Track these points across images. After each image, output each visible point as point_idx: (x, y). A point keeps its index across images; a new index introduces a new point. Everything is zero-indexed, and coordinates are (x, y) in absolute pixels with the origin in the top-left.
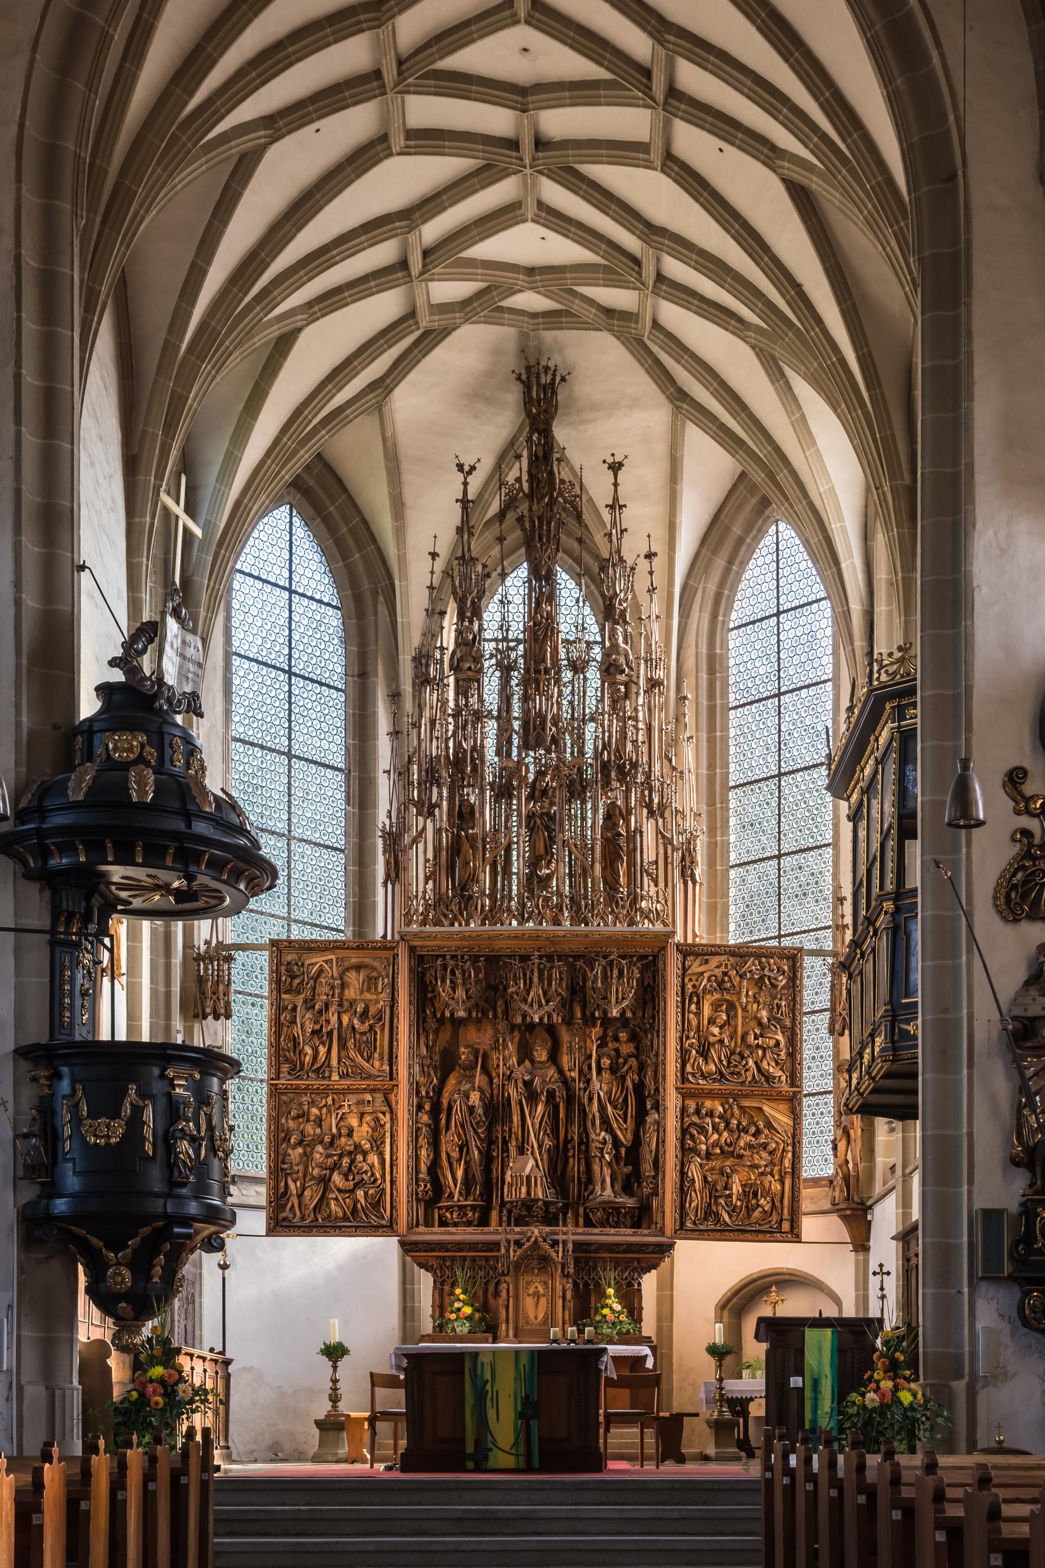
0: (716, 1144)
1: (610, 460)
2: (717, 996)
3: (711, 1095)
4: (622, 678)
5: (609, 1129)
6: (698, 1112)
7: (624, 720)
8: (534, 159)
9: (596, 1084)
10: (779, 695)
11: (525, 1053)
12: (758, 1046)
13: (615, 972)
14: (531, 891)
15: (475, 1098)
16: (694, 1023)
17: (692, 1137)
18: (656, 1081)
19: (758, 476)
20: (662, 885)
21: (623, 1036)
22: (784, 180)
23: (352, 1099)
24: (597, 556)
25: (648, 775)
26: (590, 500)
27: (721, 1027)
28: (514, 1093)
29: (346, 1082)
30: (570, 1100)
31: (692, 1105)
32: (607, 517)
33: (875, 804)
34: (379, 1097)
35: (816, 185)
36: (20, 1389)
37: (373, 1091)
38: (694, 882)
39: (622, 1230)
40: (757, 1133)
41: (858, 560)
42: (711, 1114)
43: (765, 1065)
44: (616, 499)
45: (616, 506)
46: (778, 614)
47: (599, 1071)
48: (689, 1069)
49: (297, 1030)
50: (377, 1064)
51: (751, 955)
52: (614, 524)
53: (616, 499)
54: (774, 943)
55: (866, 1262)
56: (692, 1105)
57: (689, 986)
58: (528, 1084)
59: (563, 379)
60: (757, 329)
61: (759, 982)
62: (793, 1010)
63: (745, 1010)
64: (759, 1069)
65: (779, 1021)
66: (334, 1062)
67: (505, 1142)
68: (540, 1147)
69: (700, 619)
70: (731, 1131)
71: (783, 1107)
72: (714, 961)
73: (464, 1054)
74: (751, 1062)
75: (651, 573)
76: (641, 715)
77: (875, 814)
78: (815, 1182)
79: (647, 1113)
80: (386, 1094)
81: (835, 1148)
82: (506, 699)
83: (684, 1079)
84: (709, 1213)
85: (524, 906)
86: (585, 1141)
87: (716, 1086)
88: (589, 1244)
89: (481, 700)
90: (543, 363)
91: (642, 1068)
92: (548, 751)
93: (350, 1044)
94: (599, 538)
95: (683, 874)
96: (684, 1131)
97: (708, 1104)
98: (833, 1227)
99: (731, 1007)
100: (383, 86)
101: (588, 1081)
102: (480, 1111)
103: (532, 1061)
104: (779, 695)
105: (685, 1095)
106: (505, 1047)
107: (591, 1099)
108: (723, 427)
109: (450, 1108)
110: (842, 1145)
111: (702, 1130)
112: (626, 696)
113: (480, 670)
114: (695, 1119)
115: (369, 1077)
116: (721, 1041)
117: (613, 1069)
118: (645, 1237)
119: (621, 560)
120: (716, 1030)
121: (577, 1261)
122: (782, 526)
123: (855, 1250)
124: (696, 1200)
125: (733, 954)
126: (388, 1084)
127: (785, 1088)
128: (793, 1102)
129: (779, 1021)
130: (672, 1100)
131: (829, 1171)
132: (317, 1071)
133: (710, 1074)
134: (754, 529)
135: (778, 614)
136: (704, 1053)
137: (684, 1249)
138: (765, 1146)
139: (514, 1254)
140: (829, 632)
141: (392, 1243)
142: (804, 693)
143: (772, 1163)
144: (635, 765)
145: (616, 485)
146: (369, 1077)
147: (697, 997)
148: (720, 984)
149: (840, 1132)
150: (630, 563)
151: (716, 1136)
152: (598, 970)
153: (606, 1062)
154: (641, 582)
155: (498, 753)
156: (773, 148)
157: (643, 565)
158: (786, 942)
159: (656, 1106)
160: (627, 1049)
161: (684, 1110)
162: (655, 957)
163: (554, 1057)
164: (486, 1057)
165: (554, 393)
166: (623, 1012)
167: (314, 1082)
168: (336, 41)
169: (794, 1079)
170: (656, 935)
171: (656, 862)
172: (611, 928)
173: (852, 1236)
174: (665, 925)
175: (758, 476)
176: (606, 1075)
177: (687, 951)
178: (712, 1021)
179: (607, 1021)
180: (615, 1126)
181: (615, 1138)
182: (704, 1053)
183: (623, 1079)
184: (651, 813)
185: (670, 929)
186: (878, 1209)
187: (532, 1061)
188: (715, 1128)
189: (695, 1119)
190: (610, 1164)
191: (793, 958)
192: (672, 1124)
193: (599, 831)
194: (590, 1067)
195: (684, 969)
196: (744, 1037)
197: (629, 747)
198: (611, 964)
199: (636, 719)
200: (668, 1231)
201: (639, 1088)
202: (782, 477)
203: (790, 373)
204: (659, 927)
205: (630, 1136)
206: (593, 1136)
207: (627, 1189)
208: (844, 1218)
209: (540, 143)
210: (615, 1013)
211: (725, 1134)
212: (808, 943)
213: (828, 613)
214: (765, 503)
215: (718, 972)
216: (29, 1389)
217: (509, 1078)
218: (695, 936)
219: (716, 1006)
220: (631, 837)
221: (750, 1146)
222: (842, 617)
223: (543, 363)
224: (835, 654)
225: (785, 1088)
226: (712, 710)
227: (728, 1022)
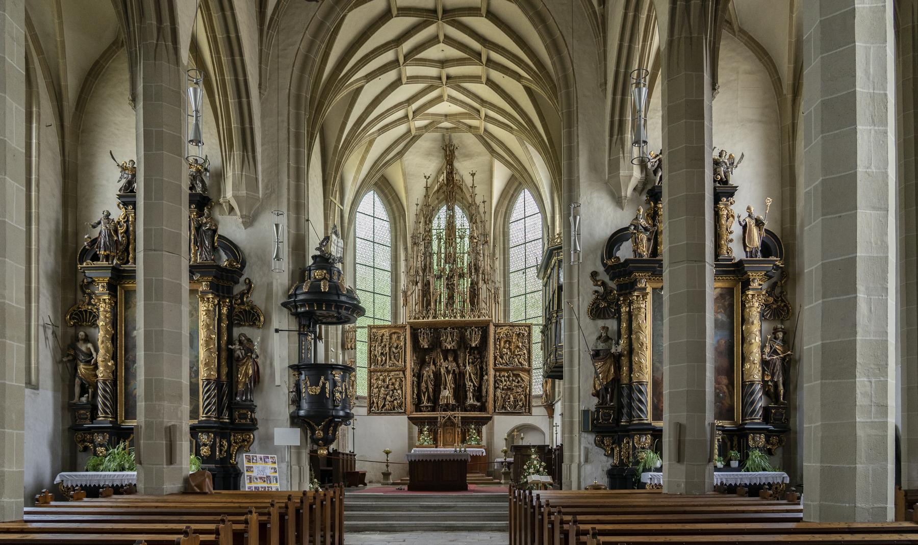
0: (505, 385)
3: (504, 370)
4: (475, 241)
5: (472, 382)
6: (500, 376)
8: (446, 82)
9: (468, 368)
10: (525, 243)
11: (446, 359)
12: (518, 355)
13: (474, 333)
14: (447, 308)
16: (498, 347)
17: (498, 384)
18: (486, 366)
19: (518, 175)
20: (488, 304)
22: (523, 86)
24: (468, 202)
28: (443, 371)
33: (551, 281)
35: (534, 87)
36: (291, 467)
38: (498, 303)
39: (476, 413)
40: (518, 382)
41: (549, 201)
42: (504, 376)
43: (520, 360)
46: (525, 218)
47: (469, 363)
49: (376, 353)
51: (516, 326)
54: (524, 322)
55: (553, 421)
57: (497, 336)
60: (516, 130)
61: (518, 335)
62: (529, 343)
64: (519, 362)
65: (525, 346)
69: (500, 220)
70: (510, 381)
72: (505, 328)
76: (481, 252)
77: (551, 284)
78: (537, 397)
79: (484, 376)
80: (404, 372)
81: (543, 386)
82: (439, 247)
83: (495, 365)
84: (504, 407)
85: (445, 312)
88: (465, 417)
89: (432, 249)
91: (482, 362)
92: (453, 264)
94: (468, 196)
96: (495, 382)
97: (503, 374)
98: (543, 411)
99: (510, 343)
100: (399, 64)
101: (465, 367)
103: (448, 361)
104: (525, 243)
105: (496, 370)
108: (506, 161)
111: (502, 382)
113: (431, 240)
116: (507, 353)
117: (473, 363)
118: (483, 415)
121: (462, 423)
122: (526, 190)
123: (549, 418)
124: (499, 404)
125: (511, 326)
127: (527, 367)
128: (529, 372)
129: (525, 346)
130: (492, 372)
131: (541, 393)
133: (504, 363)
134: (517, 191)
135: (525, 218)
136: (502, 358)
137: (497, 418)
138: (521, 386)
139: (443, 421)
140: (541, 223)
141: (404, 419)
142: (533, 242)
143: (523, 391)
147: (500, 339)
148: (506, 335)
150: (478, 204)
152: (468, 332)
154: (481, 210)
155: (437, 265)
156: (520, 75)
157: (482, 205)
158: (528, 322)
159: (487, 374)
161: (495, 375)
166: (476, 345)
168: (385, 53)
169: (530, 365)
172: (472, 319)
173: (548, 414)
174: (489, 317)
175: (518, 175)
177: (496, 326)
179: (472, 348)
181: (474, 384)
182: (502, 358)
184: (485, 282)
185: (490, 319)
186: (556, 405)
188: (505, 381)
191: (529, 327)
193: (468, 289)
195: (495, 331)
196: (514, 352)
198: (472, 330)
200: (491, 413)
201: (481, 368)
202: (525, 175)
203: (527, 144)
204: (487, 318)
205: (478, 383)
207: (478, 400)
208: (545, 408)
209: (448, 77)
210: (473, 345)
212: (534, 321)
213: (540, 217)
214: (520, 183)
215: (506, 332)
216: (293, 467)
217: (441, 366)
218: (499, 320)
219: (505, 342)
221: (516, 386)
222: (545, 218)
224: (543, 230)
225: (527, 367)
226: (504, 248)
227: (509, 348)
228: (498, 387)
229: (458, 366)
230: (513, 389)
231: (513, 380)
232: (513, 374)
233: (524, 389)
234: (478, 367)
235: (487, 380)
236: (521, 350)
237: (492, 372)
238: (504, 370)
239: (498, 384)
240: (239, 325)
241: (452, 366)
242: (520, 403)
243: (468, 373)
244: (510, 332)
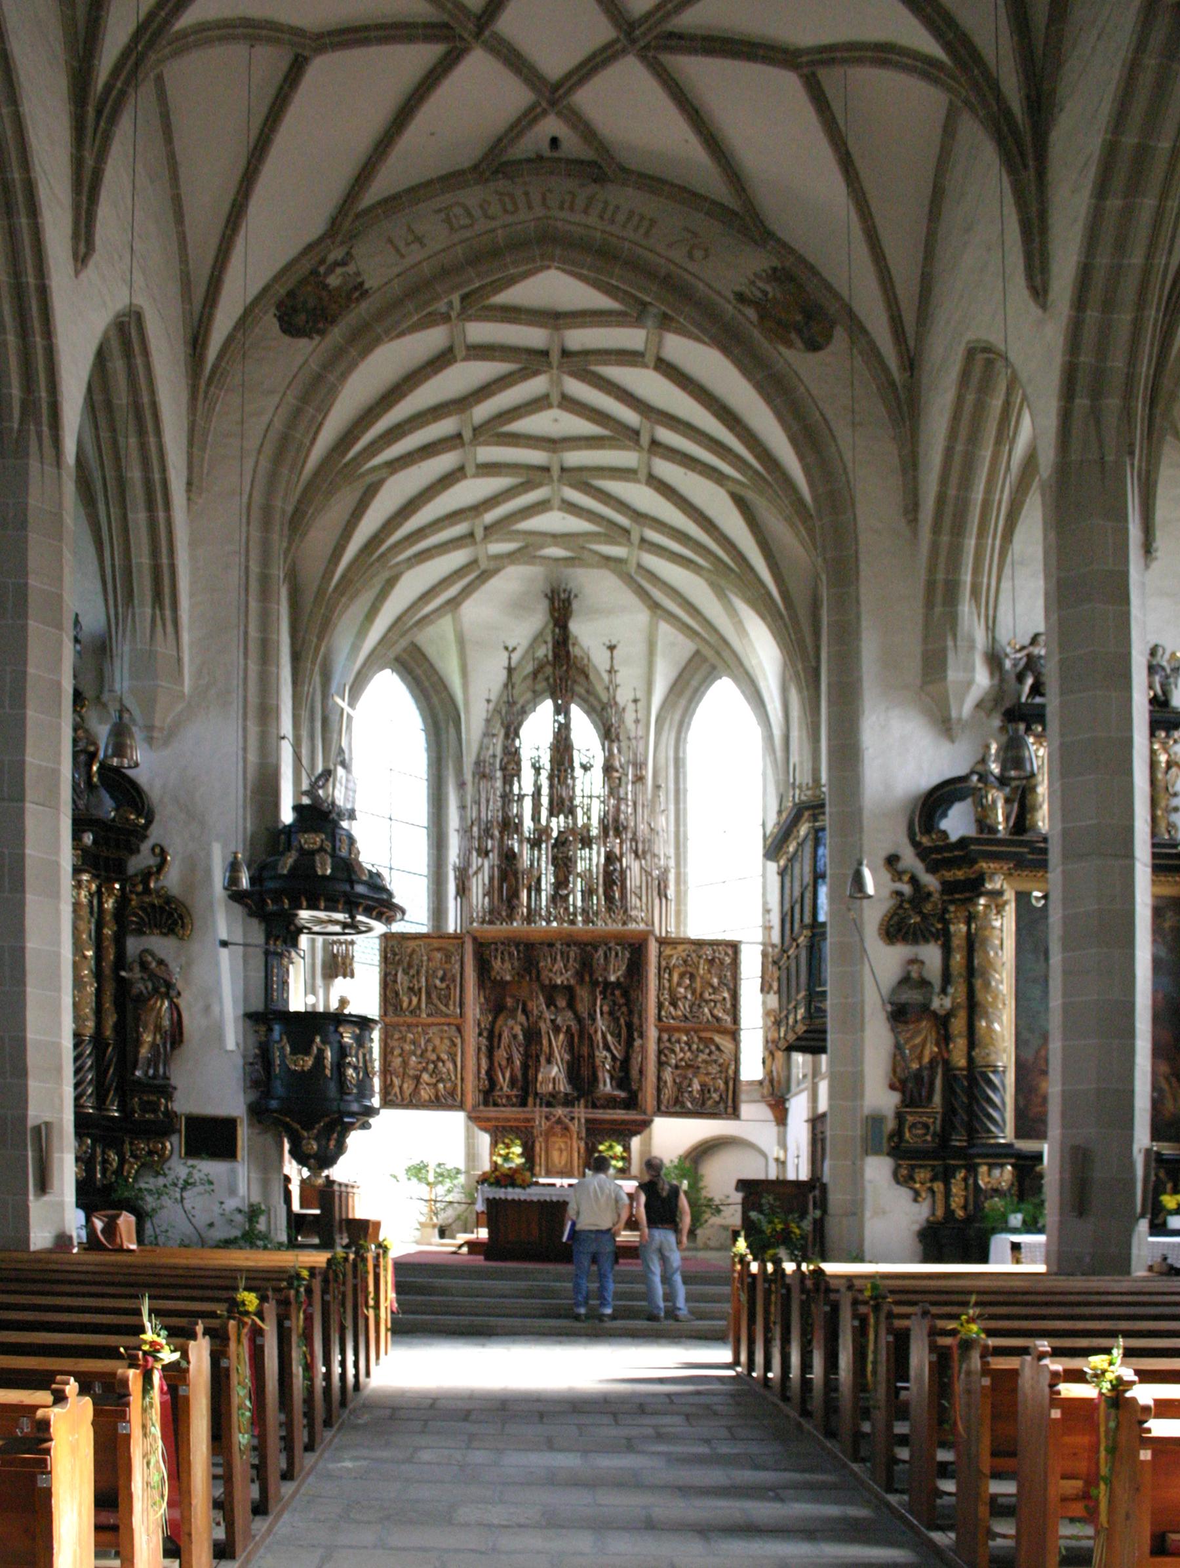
0: (682, 1060)
1: (608, 643)
2: (682, 969)
3: (678, 1029)
4: (616, 775)
6: (669, 1040)
7: (619, 799)
11: (550, 1002)
13: (613, 953)
15: (518, 1030)
17: (666, 1056)
18: (640, 1018)
21: (617, 993)
23: (435, 1029)
25: (635, 834)
26: (595, 667)
27: (686, 988)
28: (543, 1027)
29: (430, 1020)
30: (582, 1031)
31: (665, 1036)
32: (605, 676)
34: (454, 1028)
37: (449, 1024)
42: (679, 1041)
43: (716, 1012)
44: (612, 667)
45: (611, 671)
47: (602, 1013)
48: (663, 1013)
50: (452, 1008)
52: (611, 681)
53: (612, 667)
56: (665, 1036)
58: (553, 1021)
59: (576, 596)
63: (702, 978)
66: (423, 1005)
67: (538, 1057)
68: (562, 1060)
71: (728, 1038)
72: (680, 948)
73: (509, 1002)
74: (706, 1010)
75: (636, 711)
83: (660, 1019)
86: (592, 1056)
87: (683, 1024)
90: (563, 586)
91: (631, 1012)
93: (434, 996)
95: (659, 894)
96: (660, 1052)
97: (676, 1036)
99: (692, 977)
102: (521, 1037)
106: (537, 998)
107: (596, 1032)
109: (500, 1036)
110: (768, 1062)
111: (673, 1051)
112: (620, 785)
114: (668, 1044)
115: (447, 1016)
119: (616, 703)
120: (682, 990)
126: (458, 1021)
128: (734, 1035)
130: (652, 1033)
132: (411, 1012)
136: (674, 1004)
144: (625, 828)
145: (612, 658)
146: (447, 1016)
149: (767, 1054)
151: (682, 1055)
153: (606, 1009)
159: (641, 1036)
160: (622, 1001)
161: (660, 1039)
162: (640, 945)
163: (571, 1005)
164: (524, 1005)
165: (570, 604)
166: (618, 979)
167: (410, 1020)
169: (736, 1020)
170: (641, 932)
171: (641, 887)
174: (647, 924)
176: (606, 1016)
178: (679, 985)
179: (607, 984)
180: (612, 1047)
182: (674, 1004)
183: (618, 1019)
187: (556, 1006)
188: (682, 1050)
189: (668, 1044)
190: (609, 1071)
192: (652, 1047)
194: (595, 1011)
197: (622, 816)
199: (626, 799)
201: (629, 1025)
206: (597, 1053)
210: (613, 978)
211: (689, 1054)
217: (540, 1017)
220: (623, 872)
223: (563, 586)
228: (667, 1063)
229: (579, 1019)
230: (698, 1068)
231: (698, 1050)
232: (700, 1039)
233: (723, 1068)
234: (622, 1021)
235: (643, 1048)
236: (715, 990)
237: (652, 1033)
238: (678, 1029)
239: (666, 1056)
240: (140, 932)
241: (566, 1019)
242: (716, 1096)
243: (599, 1034)
244: (694, 955)
